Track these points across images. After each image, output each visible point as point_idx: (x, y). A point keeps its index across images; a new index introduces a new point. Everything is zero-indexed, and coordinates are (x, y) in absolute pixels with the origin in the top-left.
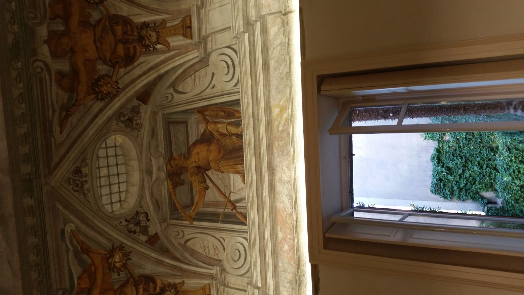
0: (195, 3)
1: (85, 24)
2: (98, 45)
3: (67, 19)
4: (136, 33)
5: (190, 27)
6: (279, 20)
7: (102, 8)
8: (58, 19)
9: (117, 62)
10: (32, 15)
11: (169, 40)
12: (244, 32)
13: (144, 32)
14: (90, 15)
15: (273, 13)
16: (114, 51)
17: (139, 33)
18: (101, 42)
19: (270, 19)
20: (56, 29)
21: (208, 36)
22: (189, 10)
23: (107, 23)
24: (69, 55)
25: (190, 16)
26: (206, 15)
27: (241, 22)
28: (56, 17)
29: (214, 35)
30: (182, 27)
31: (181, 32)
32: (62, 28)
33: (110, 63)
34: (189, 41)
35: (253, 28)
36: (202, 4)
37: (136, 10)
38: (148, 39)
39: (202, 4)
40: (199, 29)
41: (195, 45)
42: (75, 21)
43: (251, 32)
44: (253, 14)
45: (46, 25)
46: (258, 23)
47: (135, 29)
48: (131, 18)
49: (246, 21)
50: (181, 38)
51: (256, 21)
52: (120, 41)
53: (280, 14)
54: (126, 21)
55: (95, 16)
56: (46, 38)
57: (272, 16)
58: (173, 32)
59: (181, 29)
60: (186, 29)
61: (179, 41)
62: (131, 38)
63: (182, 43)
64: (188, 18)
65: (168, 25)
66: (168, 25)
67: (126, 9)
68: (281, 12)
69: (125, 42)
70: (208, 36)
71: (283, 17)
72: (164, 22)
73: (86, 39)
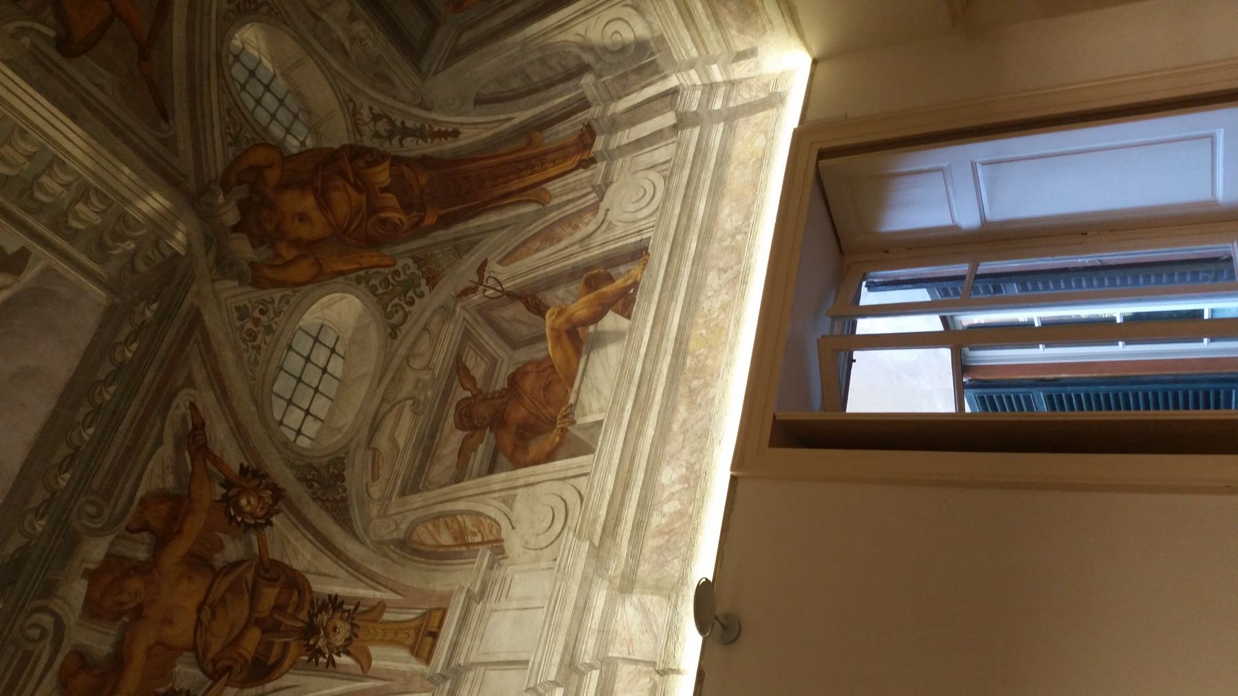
0: (468, 585)
1: (198, 561)
2: (205, 617)
3: (162, 540)
4: (303, 615)
5: (435, 636)
6: (645, 682)
7: (254, 538)
8: (145, 534)
9: (229, 669)
10: (91, 509)
11: (374, 650)
12: (556, 684)
13: (323, 618)
14: (221, 547)
15: (636, 662)
16: (236, 641)
17: (311, 616)
18: (214, 613)
19: (625, 671)
20: (129, 553)
21: (469, 667)
22: (447, 597)
23: (250, 576)
24: (126, 619)
25: (445, 611)
26: (480, 618)
27: (556, 659)
28: (145, 527)
29: (483, 669)
30: (418, 629)
31: (410, 641)
32: (142, 554)
33: (210, 668)
34: (419, 667)
35: (580, 680)
36: (482, 592)
37: (327, 564)
38: (327, 636)
39: (482, 592)
40: (455, 645)
41: (431, 680)
42: (179, 549)
43: (573, 689)
44: (588, 648)
45: (111, 538)
46: (596, 673)
47: (307, 605)
48: (310, 578)
49: (568, 658)
50: (404, 654)
51: (592, 667)
52: (259, 622)
53: (651, 669)
54: (295, 582)
55: (232, 550)
56: (92, 567)
57: (631, 667)
58: (390, 636)
59: (412, 633)
60: (423, 638)
61: (394, 659)
62: (287, 622)
63: (402, 667)
64: (439, 614)
65: (387, 616)
66: (387, 616)
67: (309, 557)
68: (654, 663)
69: (270, 627)
70: (469, 667)
71: (657, 677)
72: (381, 606)
73: (184, 596)
